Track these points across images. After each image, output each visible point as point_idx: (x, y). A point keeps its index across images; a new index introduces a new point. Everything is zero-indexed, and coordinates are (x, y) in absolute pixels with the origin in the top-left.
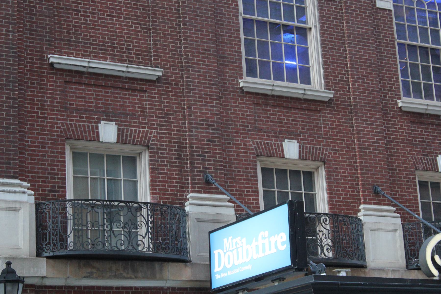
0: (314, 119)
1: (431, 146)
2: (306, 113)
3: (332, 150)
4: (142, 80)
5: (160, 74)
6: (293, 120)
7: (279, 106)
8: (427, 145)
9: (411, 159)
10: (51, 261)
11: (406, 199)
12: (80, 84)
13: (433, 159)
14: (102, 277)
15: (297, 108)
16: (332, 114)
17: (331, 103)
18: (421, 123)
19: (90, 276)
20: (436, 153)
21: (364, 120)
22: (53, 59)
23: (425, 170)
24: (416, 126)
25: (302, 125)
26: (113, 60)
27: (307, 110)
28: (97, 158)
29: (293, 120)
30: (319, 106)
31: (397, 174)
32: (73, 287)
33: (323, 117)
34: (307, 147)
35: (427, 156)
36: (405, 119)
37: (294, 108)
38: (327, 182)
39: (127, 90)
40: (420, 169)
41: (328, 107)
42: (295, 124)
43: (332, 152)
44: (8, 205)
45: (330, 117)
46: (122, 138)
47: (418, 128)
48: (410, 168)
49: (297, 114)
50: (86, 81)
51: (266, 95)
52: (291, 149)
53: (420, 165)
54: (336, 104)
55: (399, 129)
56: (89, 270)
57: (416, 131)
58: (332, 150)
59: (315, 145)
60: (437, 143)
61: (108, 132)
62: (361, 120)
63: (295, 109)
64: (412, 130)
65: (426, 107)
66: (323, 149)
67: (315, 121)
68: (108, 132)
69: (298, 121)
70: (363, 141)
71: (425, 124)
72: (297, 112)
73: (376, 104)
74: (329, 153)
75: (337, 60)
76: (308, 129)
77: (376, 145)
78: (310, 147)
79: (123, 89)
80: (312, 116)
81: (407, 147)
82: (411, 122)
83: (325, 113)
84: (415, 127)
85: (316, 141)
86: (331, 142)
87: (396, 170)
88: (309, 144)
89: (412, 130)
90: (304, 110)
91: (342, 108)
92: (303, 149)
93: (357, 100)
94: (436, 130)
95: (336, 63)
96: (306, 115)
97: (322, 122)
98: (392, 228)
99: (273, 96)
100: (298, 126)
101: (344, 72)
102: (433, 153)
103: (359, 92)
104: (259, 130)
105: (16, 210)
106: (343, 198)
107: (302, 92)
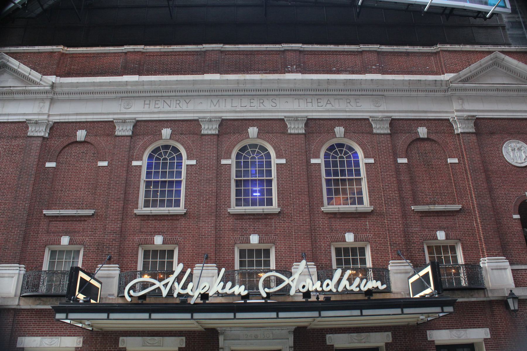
4: (85, 216)
5: (93, 212)
7: (155, 220)
10: (23, 298)
12: (56, 221)
14: (45, 304)
18: (242, 219)
19: (40, 304)
22: (45, 212)
26: (72, 209)
28: (61, 252)
32: (34, 309)
39: (78, 221)
44: (9, 275)
46: (71, 243)
50: (59, 220)
51: (149, 215)
52: (158, 240)
56: (40, 302)
61: (65, 240)
68: (65, 240)
71: (245, 219)
79: (76, 221)
98: (211, 275)
99: (153, 215)
104: (142, 232)
105: (13, 277)
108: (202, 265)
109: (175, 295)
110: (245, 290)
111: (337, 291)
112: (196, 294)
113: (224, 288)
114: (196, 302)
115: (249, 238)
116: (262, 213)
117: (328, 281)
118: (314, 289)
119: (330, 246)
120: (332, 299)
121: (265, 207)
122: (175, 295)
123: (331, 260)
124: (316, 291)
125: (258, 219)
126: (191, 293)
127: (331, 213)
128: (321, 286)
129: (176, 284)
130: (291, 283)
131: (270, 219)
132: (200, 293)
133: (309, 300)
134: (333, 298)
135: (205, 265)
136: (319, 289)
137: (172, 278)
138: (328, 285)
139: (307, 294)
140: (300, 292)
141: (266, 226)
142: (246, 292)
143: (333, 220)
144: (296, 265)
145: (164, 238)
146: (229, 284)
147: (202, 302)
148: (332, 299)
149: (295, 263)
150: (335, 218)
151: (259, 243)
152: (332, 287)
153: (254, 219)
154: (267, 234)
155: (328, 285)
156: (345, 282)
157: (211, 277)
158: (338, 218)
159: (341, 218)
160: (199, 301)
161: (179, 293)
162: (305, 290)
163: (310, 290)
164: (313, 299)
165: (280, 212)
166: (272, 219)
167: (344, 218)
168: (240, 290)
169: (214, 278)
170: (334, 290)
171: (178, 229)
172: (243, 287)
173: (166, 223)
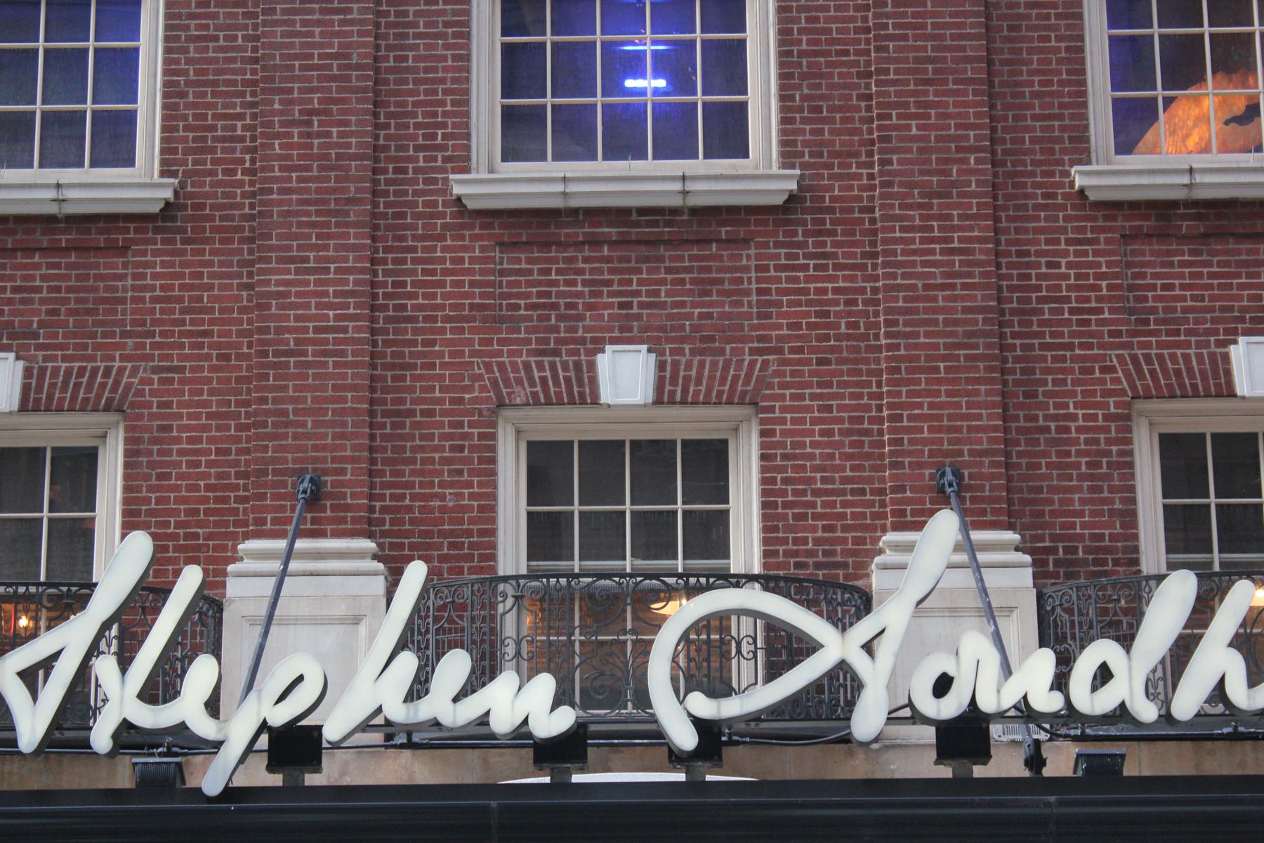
0: (100, 277)
1: (581, 318)
2: (73, 259)
3: (156, 370)
6: (15, 290)
8: (560, 318)
9: (483, 371)
11: (443, 509)
13: (578, 365)
15: (40, 249)
16: (172, 253)
17: (174, 219)
18: (546, 245)
20: (595, 340)
21: (292, 260)
23: (537, 403)
24: (523, 256)
25: (51, 301)
27: (76, 249)
29: (15, 290)
30: (127, 230)
31: (415, 425)
33: (137, 265)
34: (56, 370)
35: (556, 353)
36: (474, 238)
37: (22, 250)
38: (127, 477)
40: (518, 401)
41: (157, 230)
42: (23, 301)
43: (156, 377)
45: (163, 264)
47: (529, 261)
48: (473, 401)
49: (37, 266)
53: (517, 389)
54: (193, 218)
55: (446, 272)
57: (519, 272)
58: (156, 370)
59: (92, 359)
60: (610, 306)
62: (280, 260)
63: (29, 251)
64: (502, 273)
65: (559, 188)
66: (121, 370)
67: (101, 284)
69: (38, 290)
70: (279, 330)
72: (37, 259)
73: (349, 201)
74: (143, 381)
75: (218, 72)
76: (71, 312)
77: (331, 336)
78: (68, 372)
80: (97, 266)
81: (472, 330)
82: (501, 244)
83: (144, 253)
84: (519, 261)
85: (97, 347)
86: (155, 346)
87: (411, 413)
88: (65, 359)
89: (502, 273)
90: (68, 250)
91: (214, 229)
92: (41, 378)
93: (275, 196)
94: (608, 260)
95: (214, 83)
96: (70, 266)
97: (130, 282)
98: (342, 610)
100: (36, 306)
101: (238, 110)
102: (583, 341)
103: (281, 169)
106: (179, 525)
107: (52, 194)
108: (281, 544)
109: (101, 737)
110: (556, 705)
111: (1167, 718)
112: (238, 730)
113: (418, 689)
114: (237, 783)
115: (592, 366)
116: (677, 202)
117: (1102, 651)
118: (1009, 699)
119: (1124, 420)
120: (1129, 770)
121: (699, 165)
122: (101, 737)
123: (1129, 517)
124: (1025, 712)
125: (653, 243)
126: (204, 727)
127: (1134, 205)
128: (1061, 683)
129: (106, 667)
130: (860, 662)
131: (731, 241)
132: (264, 726)
133: (979, 771)
134: (1140, 763)
135: (300, 544)
136: (1046, 702)
137: (74, 635)
138: (1104, 675)
139: (966, 735)
140: (917, 718)
141: (704, 287)
142: (564, 719)
143: (1148, 251)
144: (897, 547)
145: (28, 373)
146: (455, 666)
147: (276, 780)
148: (1129, 770)
149: (891, 537)
150: (1163, 236)
151: (658, 401)
152: (1128, 689)
153: (623, 242)
154: (706, 343)
155: (1104, 675)
156: (1217, 659)
157: (342, 621)
158: (1184, 239)
159: (1206, 236)
160: (260, 776)
161: (126, 725)
162: (950, 707)
163: (987, 704)
164: (1005, 764)
165: (792, 198)
166: (746, 242)
167: (1222, 235)
168: (527, 703)
169: (363, 629)
170: (1147, 712)
171: (125, 315)
172: (545, 684)
173: (40, 270)
